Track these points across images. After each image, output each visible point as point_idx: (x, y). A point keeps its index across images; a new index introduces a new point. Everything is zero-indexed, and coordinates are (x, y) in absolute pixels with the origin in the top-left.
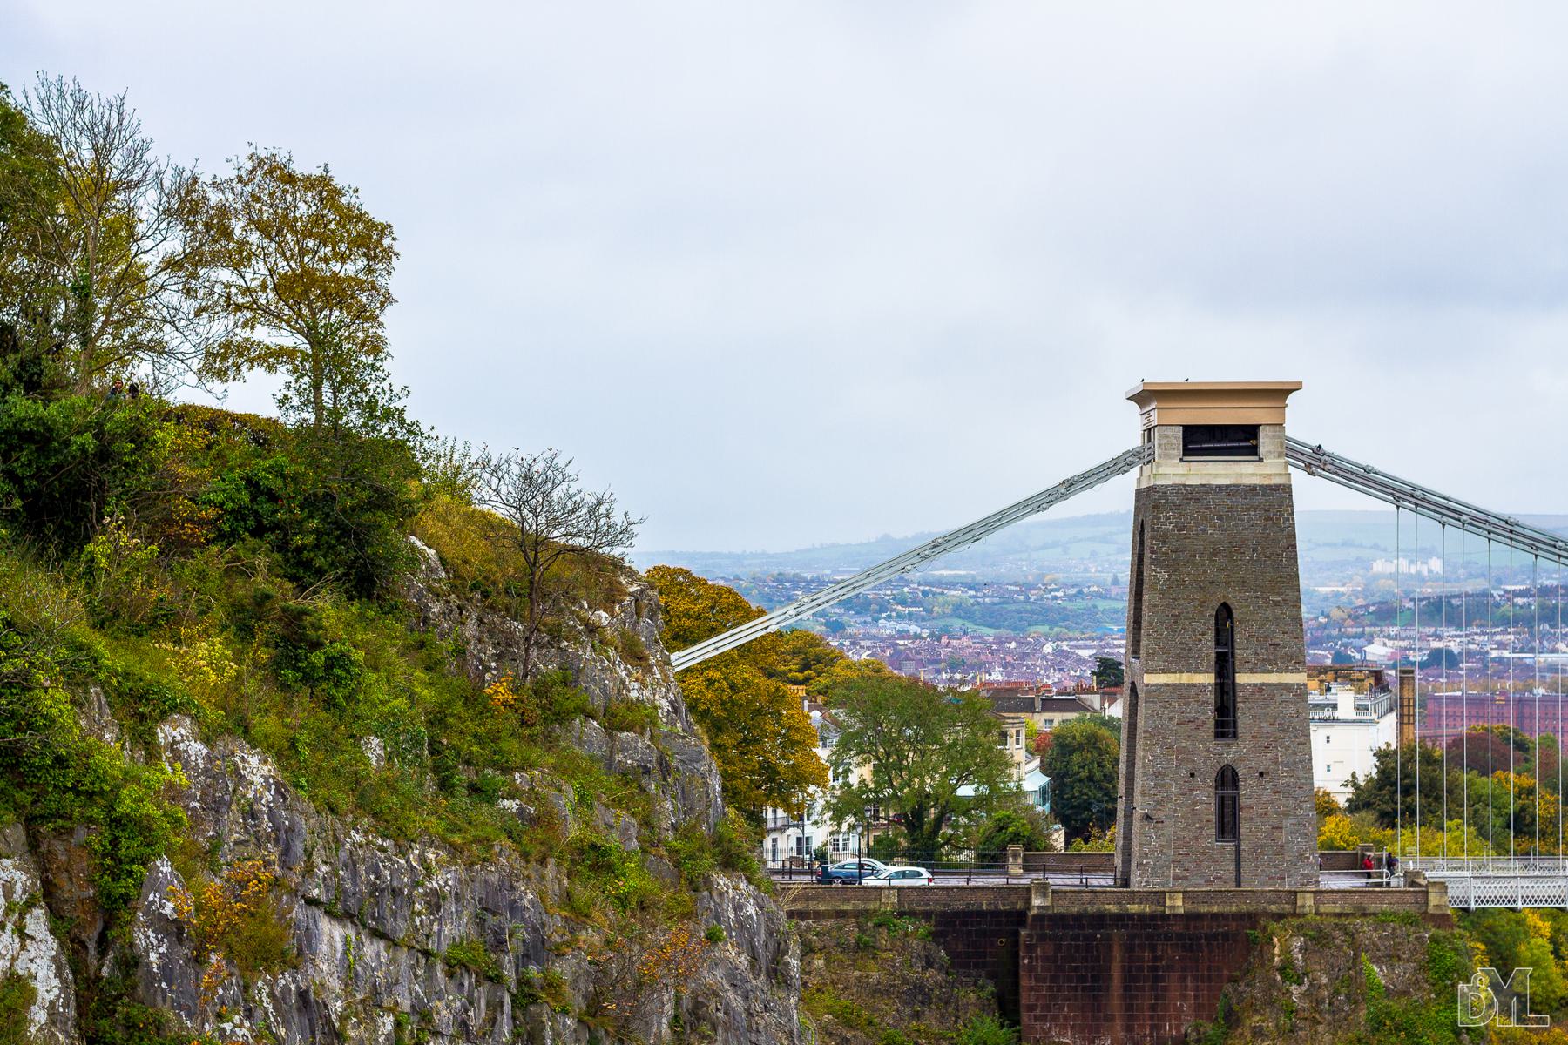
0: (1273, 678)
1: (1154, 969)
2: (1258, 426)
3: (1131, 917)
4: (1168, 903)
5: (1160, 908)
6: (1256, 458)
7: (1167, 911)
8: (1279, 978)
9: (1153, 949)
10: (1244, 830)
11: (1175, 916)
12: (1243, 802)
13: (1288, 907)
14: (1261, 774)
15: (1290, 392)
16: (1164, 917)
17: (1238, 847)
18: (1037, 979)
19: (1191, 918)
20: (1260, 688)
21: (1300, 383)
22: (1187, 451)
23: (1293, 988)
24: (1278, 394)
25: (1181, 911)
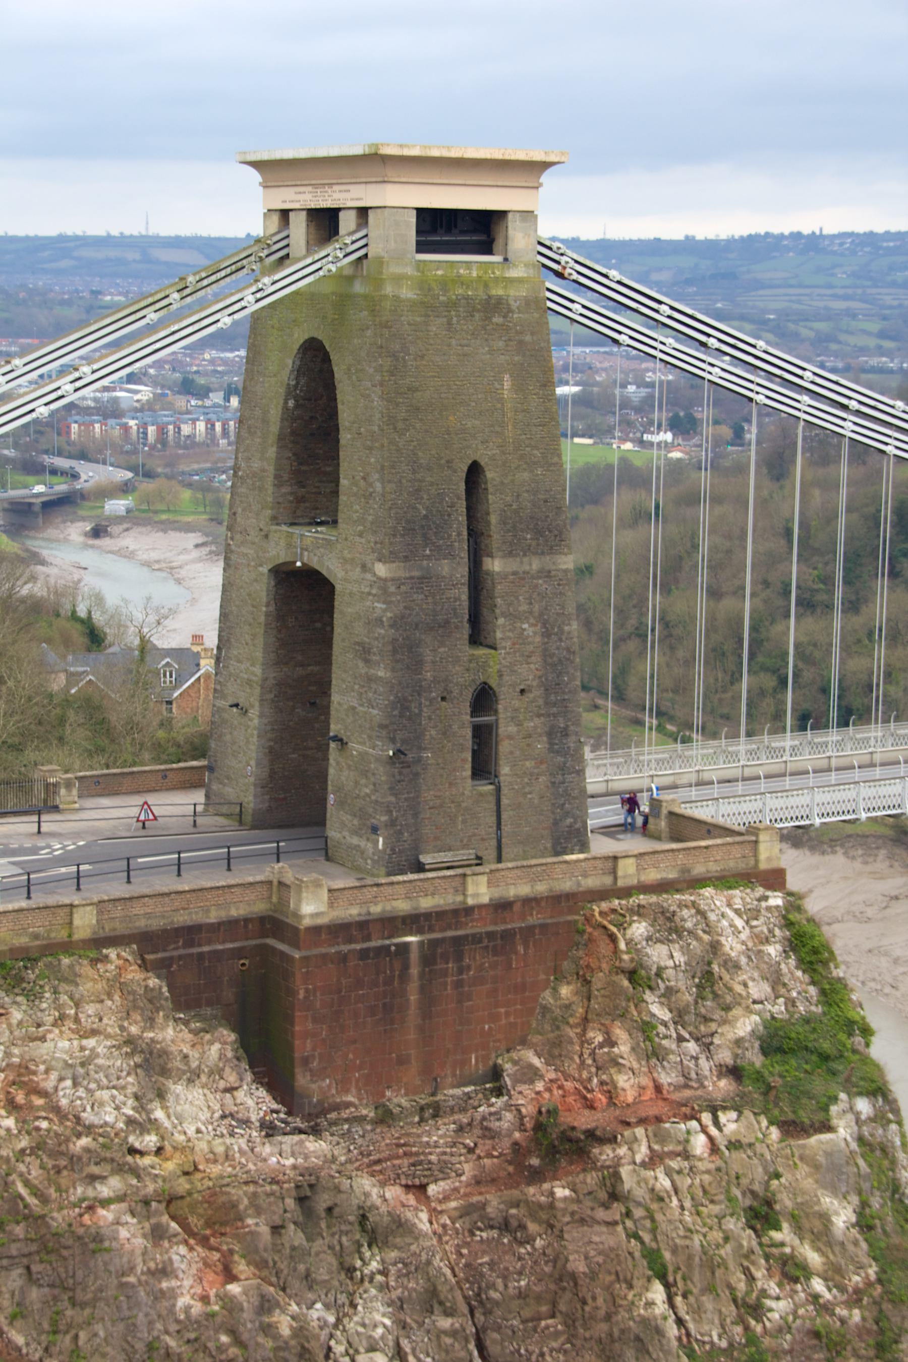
0: (535, 564)
1: (459, 984)
3: (427, 916)
4: (471, 890)
5: (459, 898)
7: (470, 901)
8: (626, 983)
9: (459, 958)
10: (505, 770)
11: (481, 907)
12: (502, 730)
13: (608, 880)
14: (522, 691)
16: (469, 911)
17: (498, 790)
18: (315, 1020)
19: (502, 907)
20: (520, 578)
22: (422, 247)
23: (648, 996)
25: (485, 900)
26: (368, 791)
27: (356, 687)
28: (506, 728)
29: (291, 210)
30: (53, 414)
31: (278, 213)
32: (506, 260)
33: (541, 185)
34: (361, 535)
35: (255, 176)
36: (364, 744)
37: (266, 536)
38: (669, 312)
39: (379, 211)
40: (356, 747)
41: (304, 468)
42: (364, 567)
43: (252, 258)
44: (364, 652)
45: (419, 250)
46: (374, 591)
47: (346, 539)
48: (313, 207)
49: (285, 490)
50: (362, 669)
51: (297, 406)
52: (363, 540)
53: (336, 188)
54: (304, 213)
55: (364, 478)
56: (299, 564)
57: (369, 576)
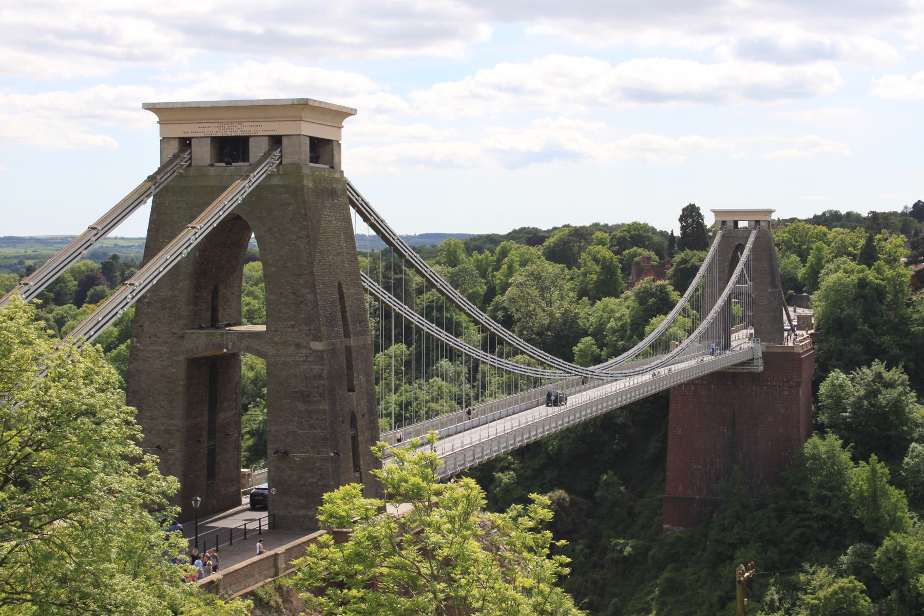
2: (328, 142)
6: (327, 167)
15: (350, 115)
21: (356, 110)
24: (339, 115)
26: (314, 480)
27: (296, 419)
28: (360, 438)
29: (193, 138)
30: (188, 253)
31: (178, 140)
32: (332, 167)
33: (343, 127)
34: (293, 327)
35: (153, 118)
36: (308, 452)
37: (182, 337)
38: (361, 202)
39: (292, 137)
40: (297, 457)
41: (197, 294)
42: (298, 346)
43: (178, 166)
44: (304, 397)
45: (311, 162)
46: (311, 359)
47: (276, 331)
48: (219, 135)
49: (191, 307)
50: (301, 406)
51: (199, 256)
52: (296, 330)
53: (244, 124)
54: (209, 139)
55: (294, 293)
56: (225, 350)
57: (305, 351)
